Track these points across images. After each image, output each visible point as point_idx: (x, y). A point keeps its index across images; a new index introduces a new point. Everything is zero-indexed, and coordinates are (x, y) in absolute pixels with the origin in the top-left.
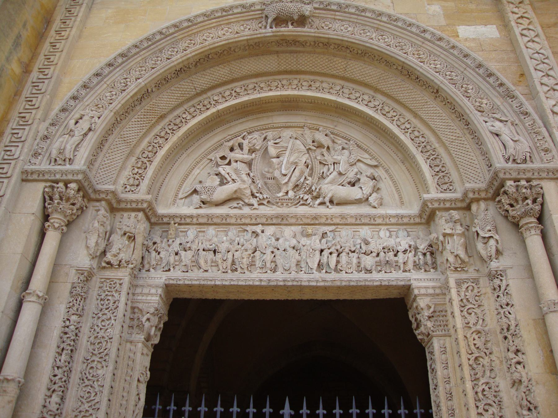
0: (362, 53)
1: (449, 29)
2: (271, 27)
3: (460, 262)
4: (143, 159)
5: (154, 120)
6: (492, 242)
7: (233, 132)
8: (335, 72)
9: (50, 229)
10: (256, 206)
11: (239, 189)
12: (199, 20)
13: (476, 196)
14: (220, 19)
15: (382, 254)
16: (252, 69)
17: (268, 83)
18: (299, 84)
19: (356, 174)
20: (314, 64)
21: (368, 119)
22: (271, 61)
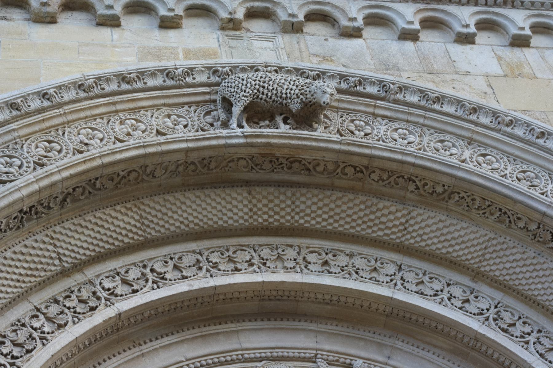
0: (445, 191)
2: (240, 126)
8: (381, 233)
12: (67, 97)
14: (117, 98)
16: (191, 218)
17: (227, 254)
18: (300, 259)
20: (332, 213)
21: (466, 340)
22: (235, 203)
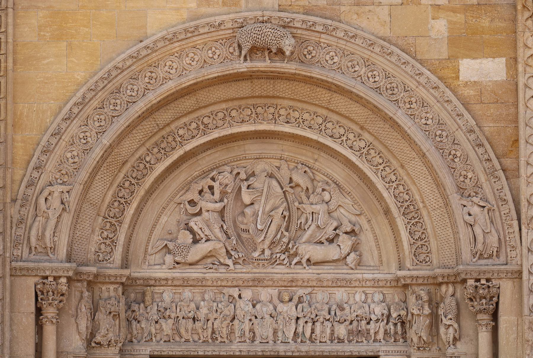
1: (450, 65)
3: (423, 342)
6: (451, 330)
10: (232, 267)
11: (214, 249)
13: (446, 280)
15: (355, 323)
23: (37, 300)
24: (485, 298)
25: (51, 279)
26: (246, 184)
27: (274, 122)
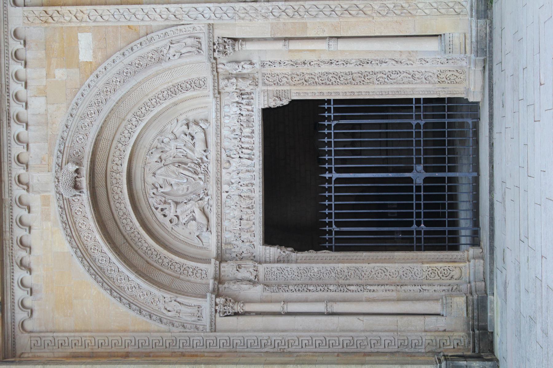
4: (182, 271)
5: (152, 267)
6: (245, 66)
7: (150, 216)
9: (244, 308)
10: (209, 197)
13: (215, 69)
19: (186, 135)
23: (230, 316)
24: (225, 46)
25: (217, 308)
26: (159, 189)
27: (121, 173)
